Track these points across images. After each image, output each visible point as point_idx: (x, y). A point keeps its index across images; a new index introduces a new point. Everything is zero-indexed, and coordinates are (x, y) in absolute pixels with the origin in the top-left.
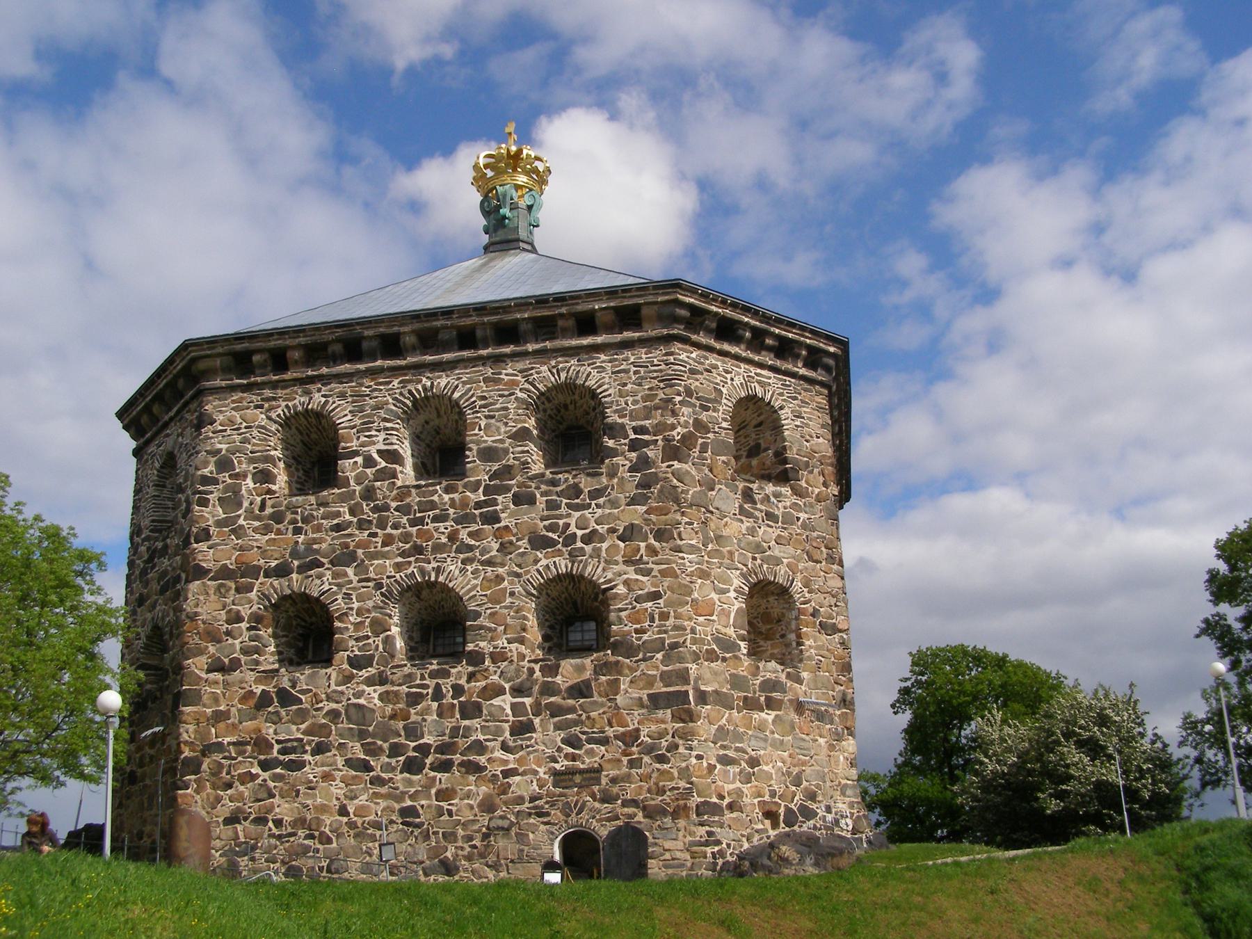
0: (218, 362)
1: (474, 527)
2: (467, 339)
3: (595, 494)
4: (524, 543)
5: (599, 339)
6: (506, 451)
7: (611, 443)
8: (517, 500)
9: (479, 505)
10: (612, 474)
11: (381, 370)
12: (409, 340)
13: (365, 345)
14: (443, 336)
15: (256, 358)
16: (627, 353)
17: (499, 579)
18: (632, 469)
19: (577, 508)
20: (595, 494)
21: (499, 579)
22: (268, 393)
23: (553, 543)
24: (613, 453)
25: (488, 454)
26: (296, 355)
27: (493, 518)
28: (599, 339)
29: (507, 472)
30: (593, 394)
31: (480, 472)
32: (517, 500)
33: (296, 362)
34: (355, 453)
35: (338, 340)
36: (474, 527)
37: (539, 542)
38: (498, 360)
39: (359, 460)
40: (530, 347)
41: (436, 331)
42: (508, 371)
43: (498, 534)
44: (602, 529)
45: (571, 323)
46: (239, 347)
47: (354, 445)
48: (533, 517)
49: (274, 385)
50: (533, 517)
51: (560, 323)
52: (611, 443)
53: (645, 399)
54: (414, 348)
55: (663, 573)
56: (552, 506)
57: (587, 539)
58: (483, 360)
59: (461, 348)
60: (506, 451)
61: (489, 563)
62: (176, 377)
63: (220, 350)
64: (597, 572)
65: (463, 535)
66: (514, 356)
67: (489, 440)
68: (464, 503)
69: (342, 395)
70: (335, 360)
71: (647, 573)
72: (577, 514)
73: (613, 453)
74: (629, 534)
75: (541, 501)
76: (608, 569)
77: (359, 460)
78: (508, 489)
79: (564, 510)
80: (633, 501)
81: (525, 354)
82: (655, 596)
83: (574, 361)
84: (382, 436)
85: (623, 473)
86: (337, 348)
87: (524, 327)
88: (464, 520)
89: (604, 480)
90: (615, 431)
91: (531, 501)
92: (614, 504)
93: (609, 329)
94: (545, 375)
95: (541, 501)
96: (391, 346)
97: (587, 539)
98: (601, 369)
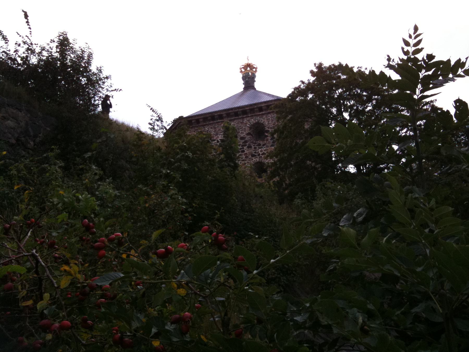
2: (236, 114)
4: (250, 156)
5: (263, 113)
6: (245, 137)
7: (267, 134)
8: (248, 147)
9: (240, 149)
10: (267, 140)
11: (219, 122)
12: (225, 115)
13: (216, 117)
15: (193, 121)
16: (269, 115)
17: (245, 164)
18: (271, 139)
19: (260, 148)
20: (263, 145)
21: (245, 164)
22: (196, 129)
23: (256, 155)
24: (267, 136)
25: (242, 138)
27: (243, 151)
28: (263, 113)
29: (246, 142)
30: (263, 124)
32: (248, 147)
34: (215, 140)
35: (210, 116)
37: (253, 156)
38: (243, 118)
39: (216, 141)
40: (249, 115)
41: (230, 113)
42: (245, 121)
43: (245, 154)
45: (257, 109)
47: (215, 138)
48: (252, 150)
49: (197, 127)
50: (252, 150)
51: (255, 110)
52: (267, 134)
54: (225, 117)
56: (255, 148)
57: (262, 154)
59: (235, 116)
60: (245, 137)
61: (243, 160)
66: (246, 117)
69: (211, 128)
70: (209, 120)
72: (260, 149)
73: (267, 136)
75: (253, 147)
77: (216, 141)
78: (246, 145)
79: (257, 149)
80: (272, 146)
81: (249, 117)
83: (258, 117)
84: (220, 136)
86: (210, 118)
87: (248, 111)
89: (265, 142)
90: (267, 131)
92: (267, 147)
93: (266, 110)
94: (253, 121)
95: (253, 147)
98: (264, 119)
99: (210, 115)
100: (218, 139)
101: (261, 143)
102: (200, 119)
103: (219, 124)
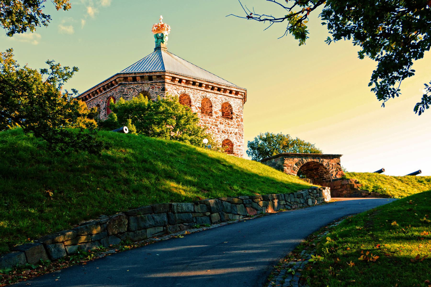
0: (169, 77)
1: (214, 126)
3: (232, 125)
8: (220, 123)
14: (210, 86)
22: (178, 87)
25: (216, 113)
26: (184, 81)
30: (230, 106)
31: (214, 116)
32: (220, 123)
33: (183, 82)
36: (214, 126)
44: (233, 132)
46: (175, 76)
48: (222, 127)
50: (222, 127)
53: (238, 109)
55: (241, 142)
56: (226, 126)
58: (215, 93)
62: (154, 75)
63: (170, 75)
64: (231, 139)
65: (212, 127)
67: (216, 110)
68: (212, 122)
69: (191, 92)
71: (239, 141)
74: (236, 134)
76: (233, 140)
80: (236, 128)
82: (240, 146)
84: (198, 103)
85: (235, 122)
88: (212, 125)
91: (223, 124)
96: (201, 85)
97: (231, 133)
99: (194, 80)
100: (197, 106)
101: (230, 122)
102: (184, 79)
103: (198, 91)
